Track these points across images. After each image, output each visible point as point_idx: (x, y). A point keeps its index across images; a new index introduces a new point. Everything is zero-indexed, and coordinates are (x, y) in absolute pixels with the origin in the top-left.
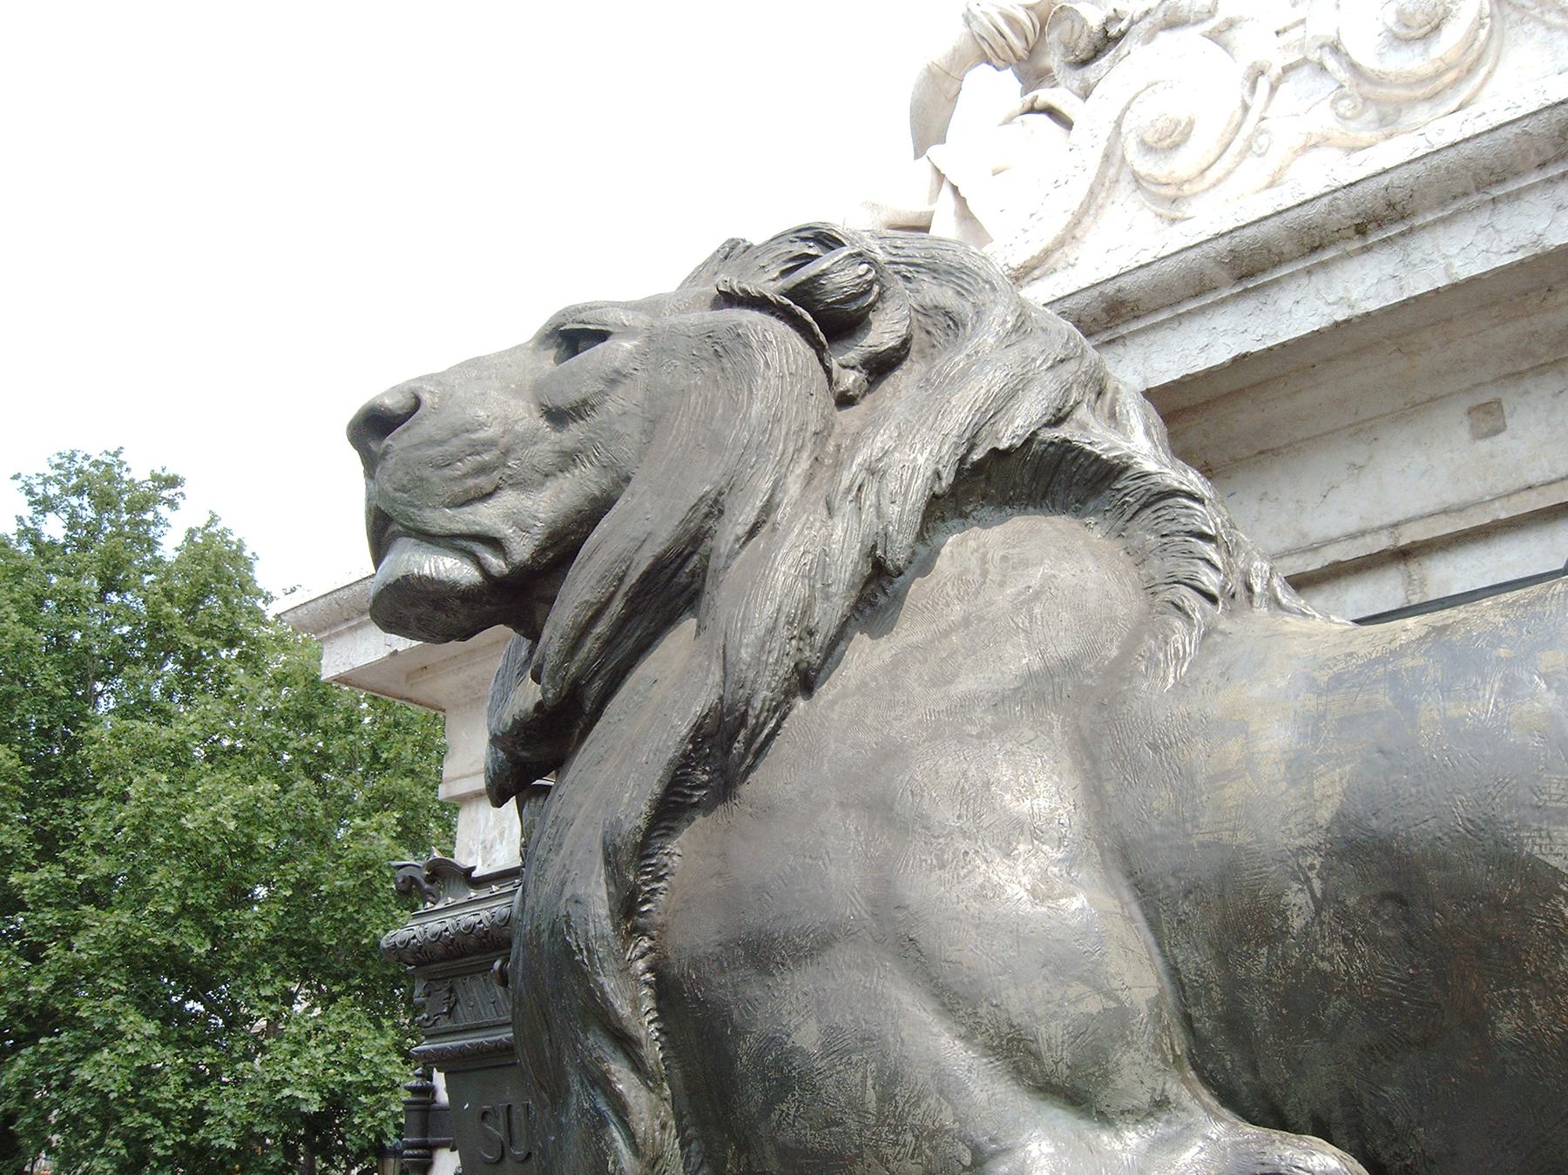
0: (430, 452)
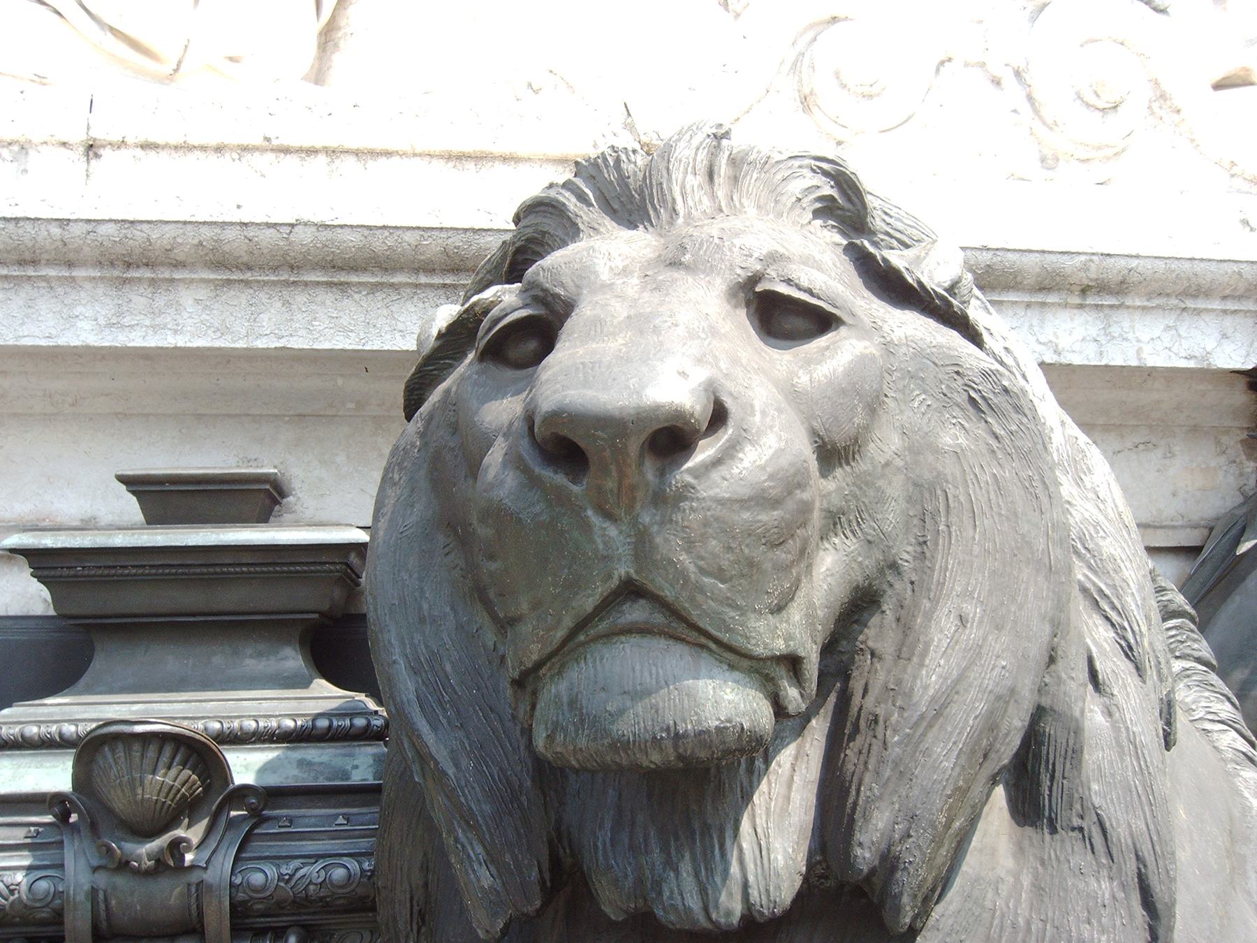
0: (764, 517)
